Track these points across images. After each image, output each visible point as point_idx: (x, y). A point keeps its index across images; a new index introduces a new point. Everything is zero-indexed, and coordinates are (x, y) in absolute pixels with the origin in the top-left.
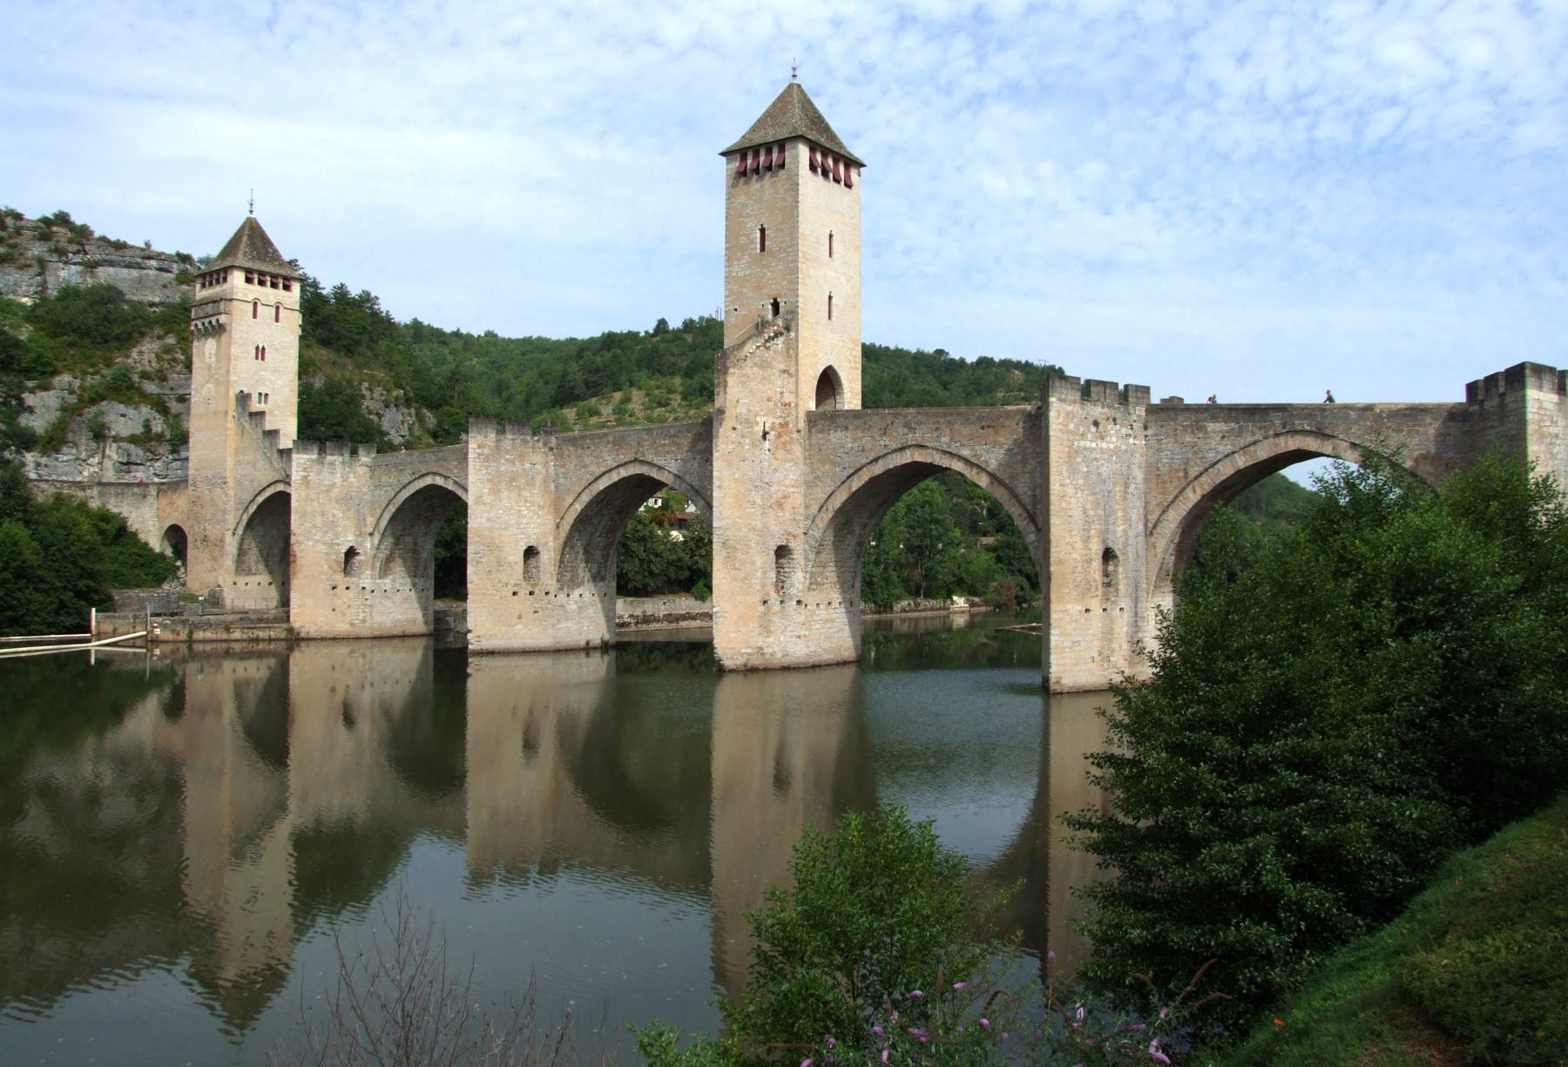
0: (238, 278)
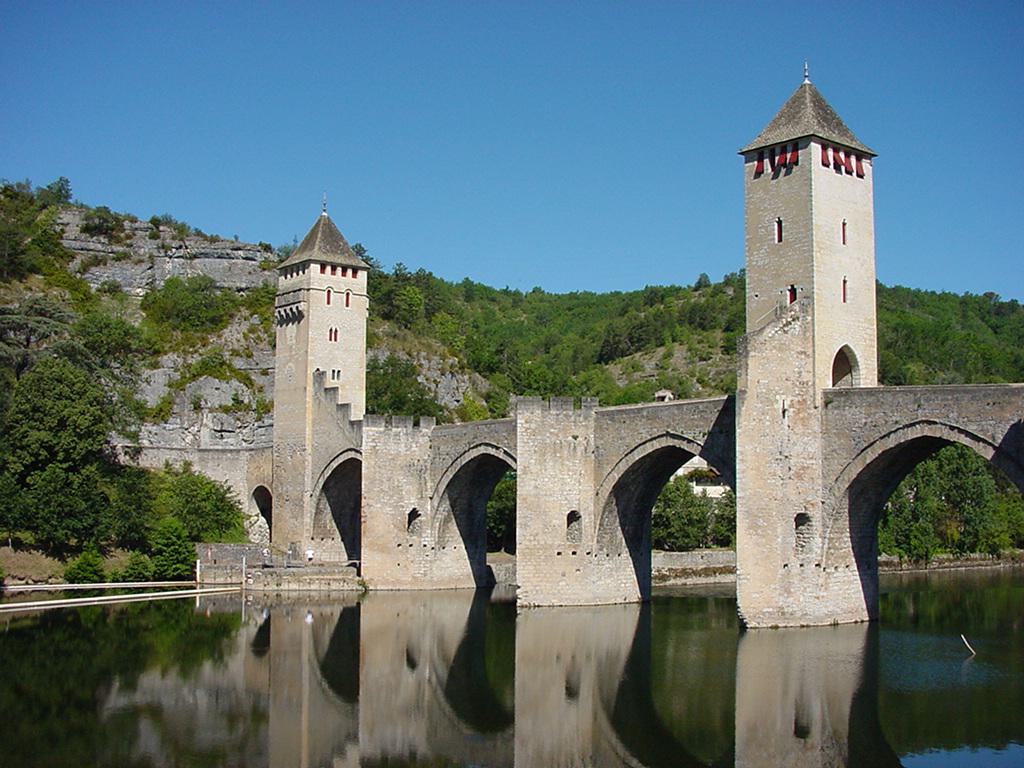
0: (315, 268)
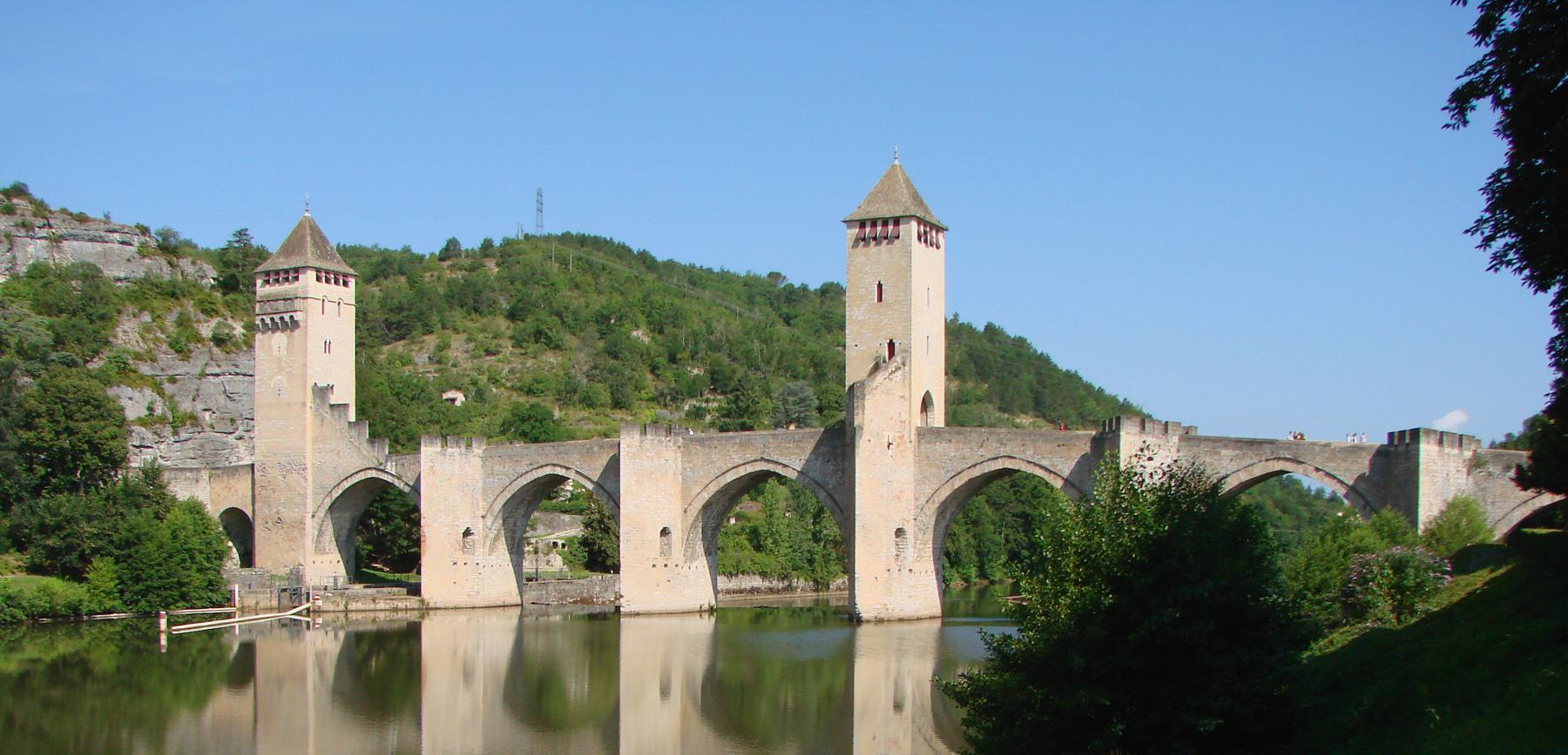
0: (312, 274)
